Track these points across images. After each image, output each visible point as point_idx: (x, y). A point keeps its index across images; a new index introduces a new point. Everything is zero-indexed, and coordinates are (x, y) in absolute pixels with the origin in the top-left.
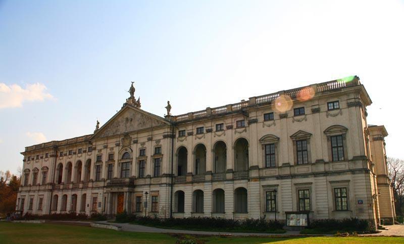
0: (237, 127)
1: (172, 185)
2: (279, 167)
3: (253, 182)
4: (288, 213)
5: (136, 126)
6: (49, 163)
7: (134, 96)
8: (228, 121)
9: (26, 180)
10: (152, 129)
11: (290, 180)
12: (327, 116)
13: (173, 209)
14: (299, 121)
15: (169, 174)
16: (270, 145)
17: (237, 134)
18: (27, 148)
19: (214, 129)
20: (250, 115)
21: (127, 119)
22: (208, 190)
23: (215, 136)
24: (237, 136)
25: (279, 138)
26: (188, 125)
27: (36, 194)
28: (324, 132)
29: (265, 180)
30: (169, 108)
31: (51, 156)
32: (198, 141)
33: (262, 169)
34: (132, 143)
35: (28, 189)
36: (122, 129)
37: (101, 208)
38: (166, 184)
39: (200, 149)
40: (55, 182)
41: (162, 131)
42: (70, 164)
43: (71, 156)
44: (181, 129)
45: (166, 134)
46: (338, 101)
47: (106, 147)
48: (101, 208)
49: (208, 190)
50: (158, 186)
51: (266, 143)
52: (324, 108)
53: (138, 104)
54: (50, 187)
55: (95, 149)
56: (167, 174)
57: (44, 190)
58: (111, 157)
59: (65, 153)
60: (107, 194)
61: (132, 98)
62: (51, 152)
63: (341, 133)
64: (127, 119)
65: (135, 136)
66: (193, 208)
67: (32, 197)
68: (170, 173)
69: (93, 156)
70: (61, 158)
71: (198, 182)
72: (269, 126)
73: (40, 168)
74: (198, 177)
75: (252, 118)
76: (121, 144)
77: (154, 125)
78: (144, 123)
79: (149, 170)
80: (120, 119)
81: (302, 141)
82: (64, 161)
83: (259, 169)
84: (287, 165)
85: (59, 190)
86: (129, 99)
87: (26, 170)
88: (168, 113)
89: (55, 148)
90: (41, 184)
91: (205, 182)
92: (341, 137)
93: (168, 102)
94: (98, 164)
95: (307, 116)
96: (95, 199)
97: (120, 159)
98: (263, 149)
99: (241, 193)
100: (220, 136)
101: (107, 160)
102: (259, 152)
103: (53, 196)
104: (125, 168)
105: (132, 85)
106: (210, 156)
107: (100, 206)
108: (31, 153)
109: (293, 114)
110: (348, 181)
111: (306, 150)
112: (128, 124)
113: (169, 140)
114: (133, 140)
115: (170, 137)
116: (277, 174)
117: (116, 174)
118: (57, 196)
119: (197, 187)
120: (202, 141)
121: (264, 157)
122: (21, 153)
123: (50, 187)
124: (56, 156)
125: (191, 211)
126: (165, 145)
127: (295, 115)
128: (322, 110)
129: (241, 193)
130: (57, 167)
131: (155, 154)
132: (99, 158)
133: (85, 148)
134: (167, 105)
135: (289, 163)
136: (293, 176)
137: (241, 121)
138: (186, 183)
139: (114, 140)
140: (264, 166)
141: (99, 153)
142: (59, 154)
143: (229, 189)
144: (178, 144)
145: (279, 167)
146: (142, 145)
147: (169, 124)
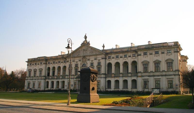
0: (133, 57)
1: (106, 78)
2: (149, 73)
3: (139, 78)
4: (152, 89)
5: (88, 53)
6: (43, 67)
7: (87, 40)
8: (129, 54)
9: (30, 74)
10: (96, 55)
11: (153, 77)
12: (167, 55)
13: (106, 87)
14: (157, 56)
15: (104, 74)
16: (146, 64)
17: (133, 59)
18: (29, 59)
19: (123, 56)
20: (138, 53)
22: (121, 80)
23: (123, 60)
24: (133, 60)
25: (149, 62)
26: (112, 54)
27: (36, 81)
28: (166, 61)
29: (143, 77)
30: (104, 46)
31: (44, 64)
32: (116, 61)
33: (143, 73)
34: (87, 60)
35: (32, 78)
36: (82, 54)
37: (73, 87)
38: (103, 77)
39: (117, 64)
40: (46, 75)
41: (101, 56)
42: (54, 68)
43: (54, 64)
44: (109, 56)
45: (103, 57)
46: (171, 50)
48: (73, 87)
49: (121, 80)
50: (100, 78)
51: (144, 63)
52: (166, 52)
53: (88, 44)
54: (44, 78)
56: (103, 74)
57: (41, 79)
59: (51, 62)
60: (76, 81)
61: (86, 40)
62: (44, 62)
63: (171, 62)
64: (84, 50)
65: (89, 57)
66: (115, 87)
67: (34, 82)
68: (105, 73)
69: (67, 65)
70: (49, 65)
71: (117, 77)
72: (145, 57)
73: (38, 69)
74: (117, 74)
75: (139, 54)
76: (81, 60)
77: (97, 53)
78: (92, 52)
80: (80, 49)
81: (157, 63)
82: (51, 66)
83: (142, 73)
84: (152, 72)
85: (49, 79)
86: (84, 41)
87: (29, 69)
88: (103, 49)
89: (46, 60)
90: (39, 76)
91: (119, 77)
92: (171, 63)
93: (104, 44)
95: (160, 55)
96: (69, 83)
97: (81, 66)
98: (143, 65)
99: (134, 82)
100: (126, 59)
101: (75, 67)
102: (141, 66)
103: (46, 82)
105: (85, 35)
106: (121, 67)
107: (72, 86)
108: (31, 62)
109: (154, 54)
110: (173, 78)
111: (159, 67)
112: (85, 52)
113: (104, 60)
114: (87, 59)
115: (105, 59)
116: (148, 75)
118: (48, 82)
119: (116, 79)
120: (118, 61)
121: (143, 69)
122: (26, 62)
123: (44, 78)
124: (46, 64)
125: (114, 88)
126: (103, 62)
127: (155, 54)
128: (165, 53)
129: (134, 82)
130: (47, 69)
131: (98, 65)
132: (70, 66)
133: (62, 61)
134: (103, 45)
135: (152, 71)
136: (154, 76)
137: (134, 54)
138: (112, 77)
139: (78, 58)
140: (143, 72)
142: (48, 63)
143: (129, 80)
144: (108, 62)
145: (149, 73)
146: (91, 61)
147: (105, 54)
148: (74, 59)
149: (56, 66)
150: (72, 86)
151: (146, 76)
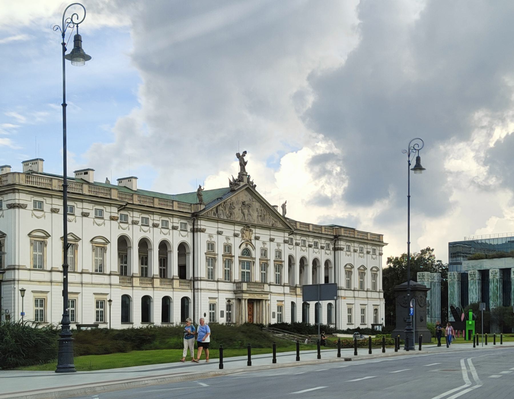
6: (112, 231)
21: (243, 203)
34: (253, 238)
55: (203, 231)
58: (228, 248)
64: (243, 203)
148: (220, 225)
149: (156, 237)
150: (222, 316)
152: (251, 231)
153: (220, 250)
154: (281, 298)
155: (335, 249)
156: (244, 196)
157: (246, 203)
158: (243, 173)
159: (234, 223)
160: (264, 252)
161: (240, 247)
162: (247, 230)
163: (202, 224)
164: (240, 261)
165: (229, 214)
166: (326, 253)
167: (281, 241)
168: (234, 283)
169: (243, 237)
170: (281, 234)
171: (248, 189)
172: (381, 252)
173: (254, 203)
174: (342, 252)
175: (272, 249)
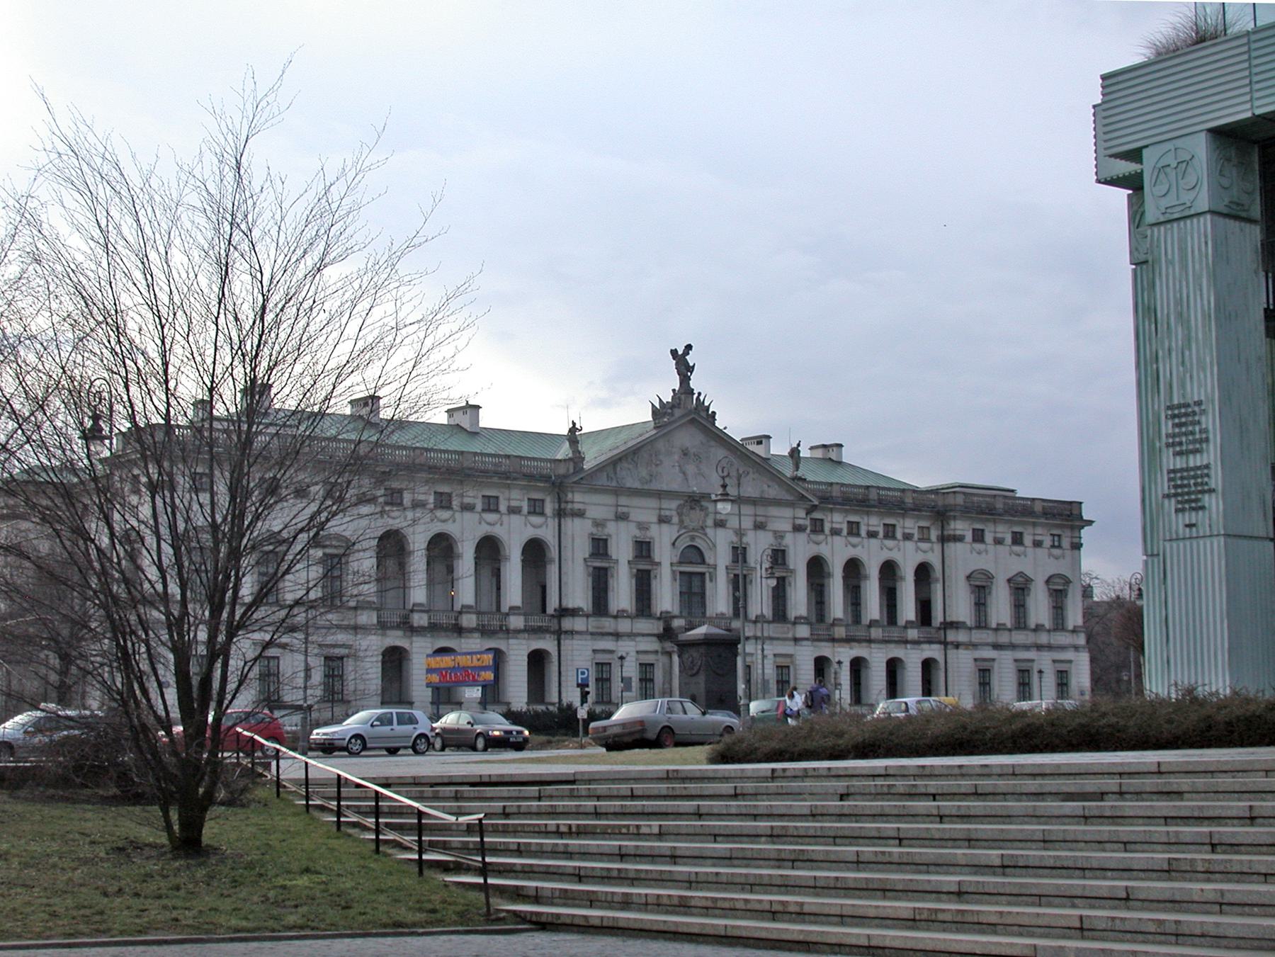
21: (685, 453)
34: (710, 522)
47: (621, 517)
55: (580, 514)
58: (643, 549)
64: (685, 453)
77: (773, 492)
79: (760, 602)
94: (598, 564)
97: (675, 560)
104: (693, 591)
110: (1070, 662)
117: (666, 597)
141: (594, 530)
151: (987, 644)
152: (702, 509)
153: (622, 551)
154: (787, 648)
155: (944, 539)
156: (688, 438)
157: (693, 450)
158: (685, 389)
159: (660, 495)
160: (739, 553)
161: (674, 544)
162: (692, 508)
163: (578, 499)
164: (673, 572)
165: (648, 477)
166: (918, 549)
167: (786, 526)
168: (659, 619)
169: (681, 522)
170: (788, 512)
171: (693, 421)
172: (1076, 540)
173: (713, 450)
174: (959, 545)
175: (758, 546)
